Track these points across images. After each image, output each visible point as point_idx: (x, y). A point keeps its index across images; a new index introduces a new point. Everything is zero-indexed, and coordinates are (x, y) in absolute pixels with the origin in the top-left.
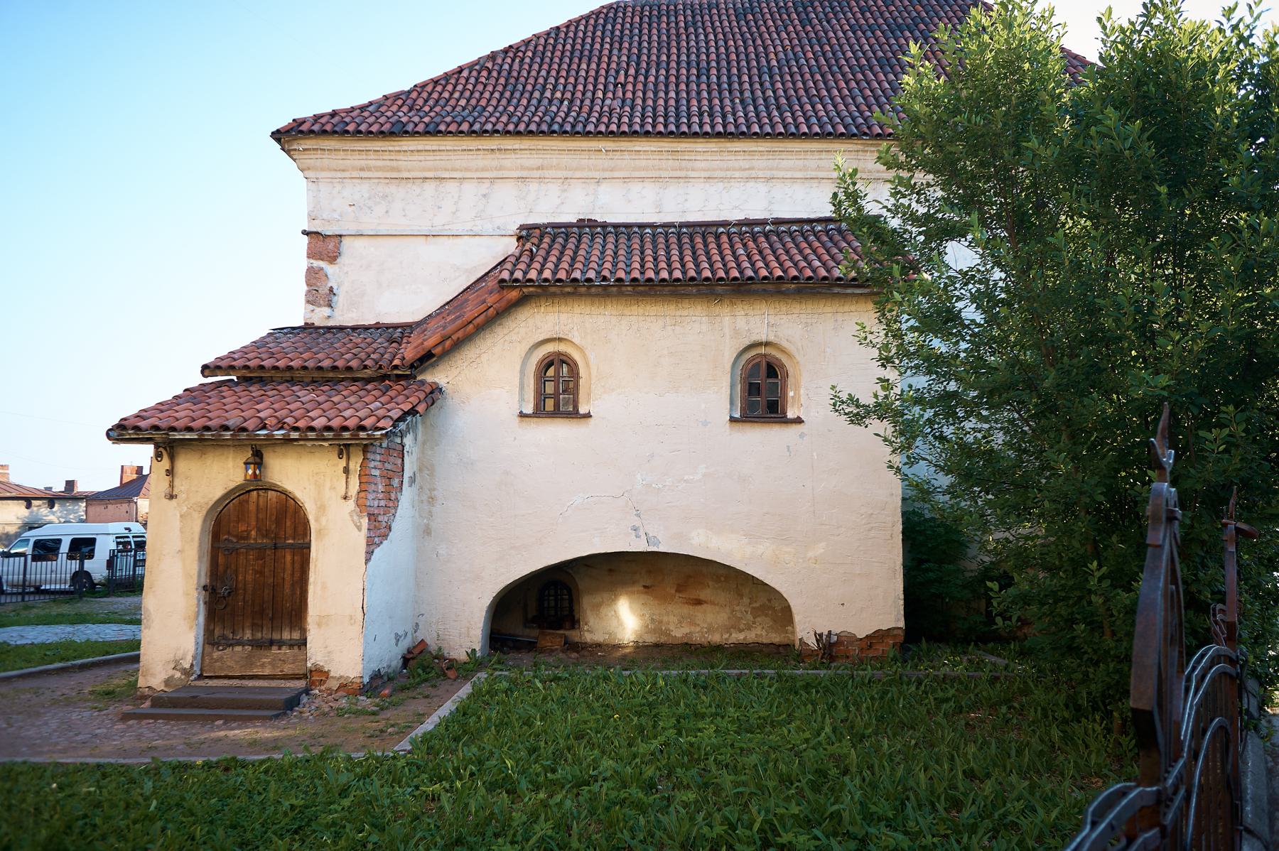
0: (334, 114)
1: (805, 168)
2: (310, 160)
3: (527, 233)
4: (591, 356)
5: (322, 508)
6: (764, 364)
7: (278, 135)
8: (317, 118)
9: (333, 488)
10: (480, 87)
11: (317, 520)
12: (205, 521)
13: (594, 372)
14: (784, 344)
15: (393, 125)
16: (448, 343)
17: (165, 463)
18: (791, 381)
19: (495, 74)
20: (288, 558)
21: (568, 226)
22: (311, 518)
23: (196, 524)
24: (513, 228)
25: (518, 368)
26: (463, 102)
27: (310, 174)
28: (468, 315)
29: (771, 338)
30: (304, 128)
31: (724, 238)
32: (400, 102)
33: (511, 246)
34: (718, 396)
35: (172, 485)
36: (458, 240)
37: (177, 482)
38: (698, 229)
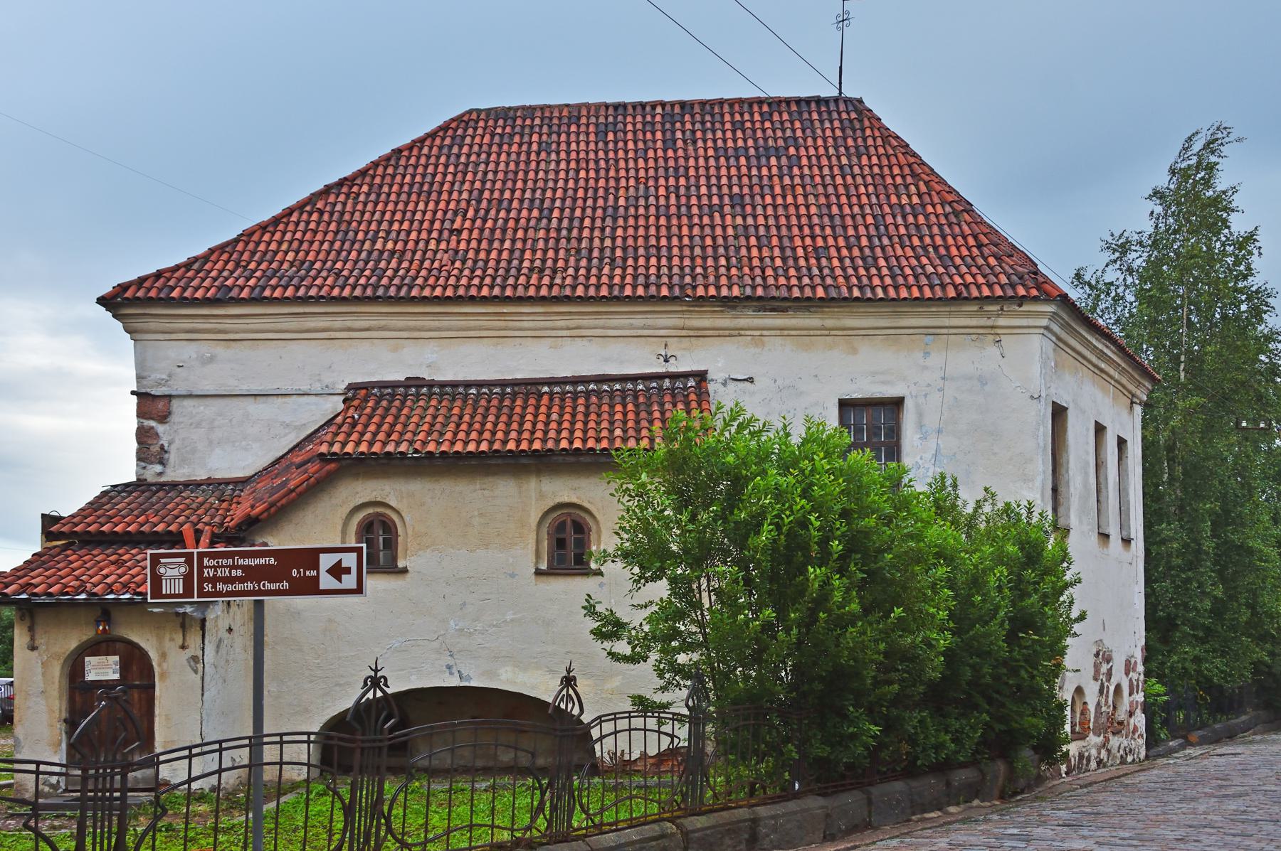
0: (159, 275)
1: (632, 327)
2: (138, 324)
3: (357, 393)
4: (407, 519)
5: (163, 656)
6: (569, 522)
7: (102, 301)
8: (141, 281)
9: (172, 640)
10: (308, 236)
11: (159, 665)
12: (63, 668)
13: (410, 532)
14: (586, 505)
15: (219, 288)
16: (273, 509)
17: (28, 619)
18: (593, 536)
19: (326, 217)
20: (136, 696)
21: (394, 385)
22: (155, 664)
23: (56, 670)
24: (342, 387)
25: (340, 528)
26: (290, 256)
27: (138, 336)
28: (291, 485)
29: (574, 500)
30: (128, 294)
31: (545, 400)
32: (225, 257)
33: (337, 404)
34: (526, 553)
35: (33, 638)
36: (287, 399)
37: (37, 636)
38: (523, 389)
